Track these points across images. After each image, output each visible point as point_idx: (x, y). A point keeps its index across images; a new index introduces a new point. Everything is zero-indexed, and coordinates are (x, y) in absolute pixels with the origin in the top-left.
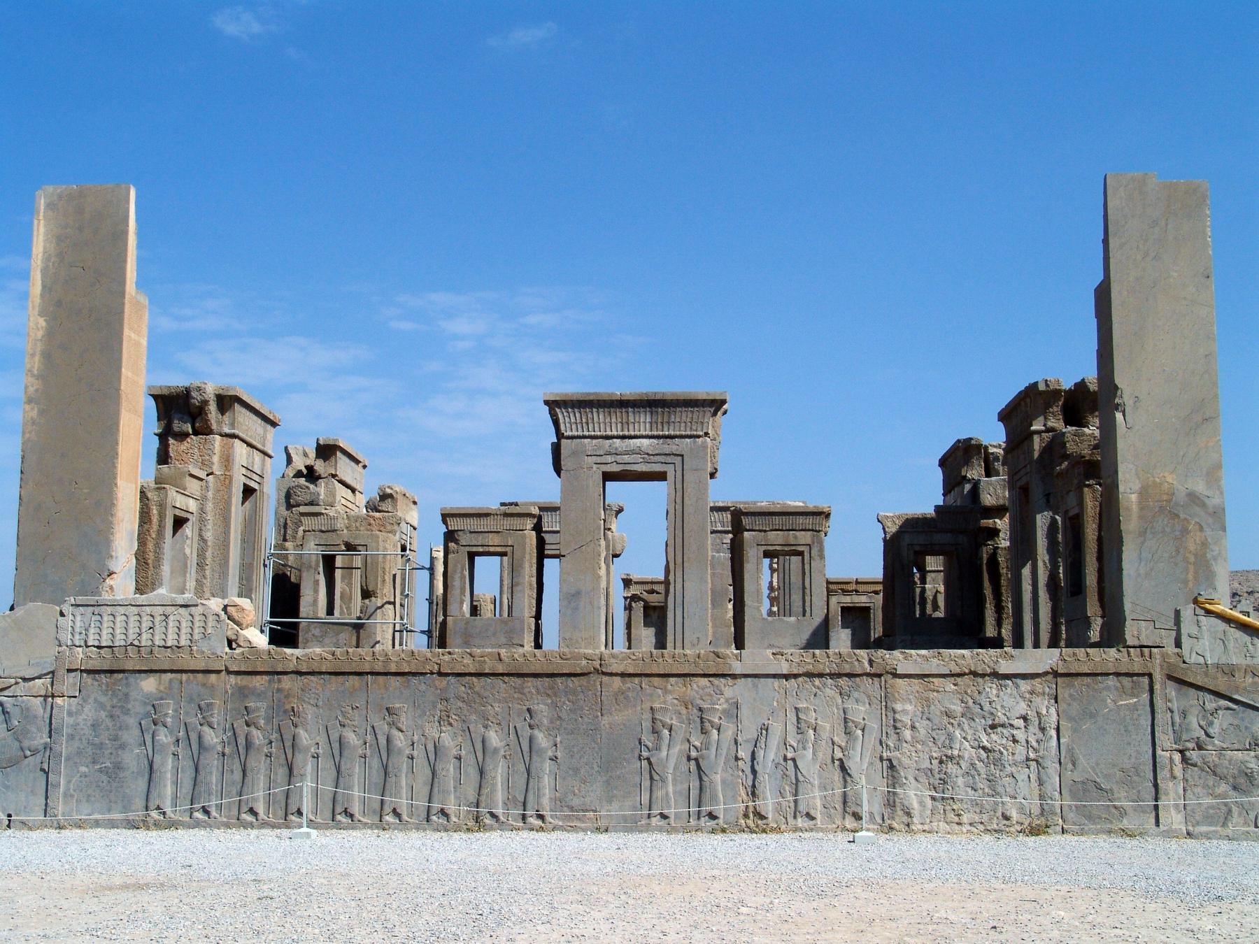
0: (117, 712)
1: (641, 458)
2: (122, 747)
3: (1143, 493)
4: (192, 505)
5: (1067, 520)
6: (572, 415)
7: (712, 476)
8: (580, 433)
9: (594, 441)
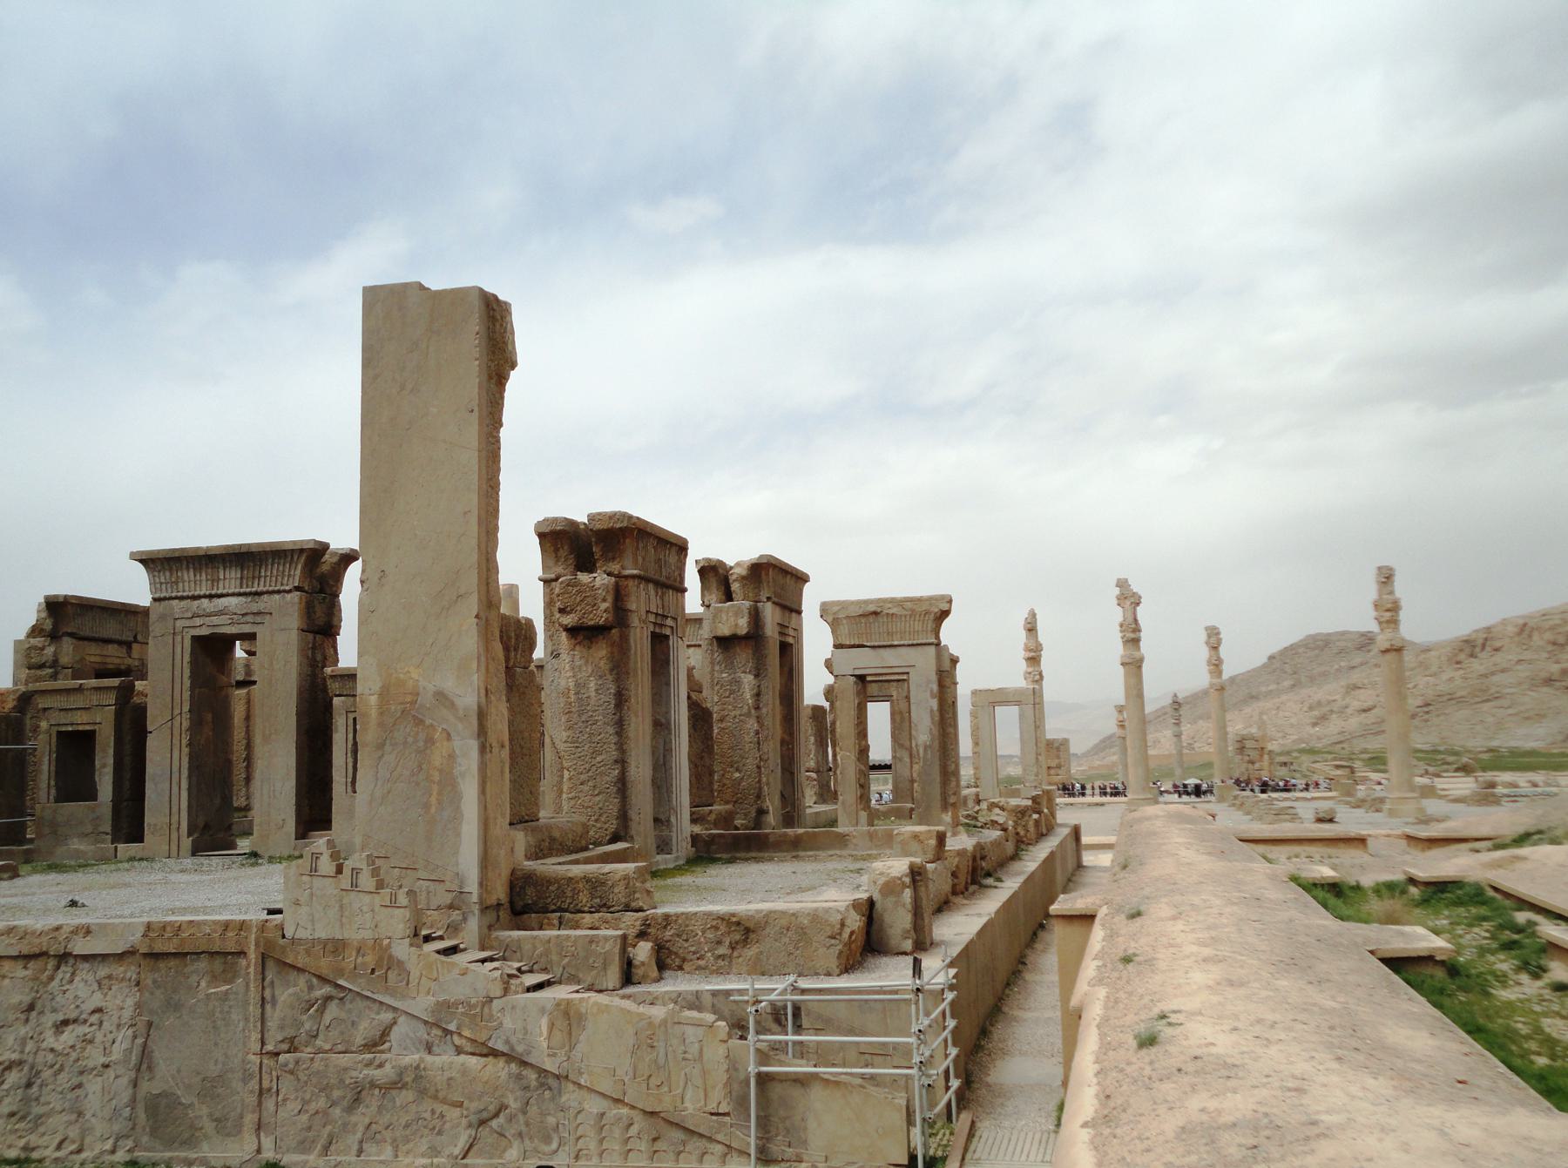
3: (384, 694)
8: (168, 596)
9: (184, 603)
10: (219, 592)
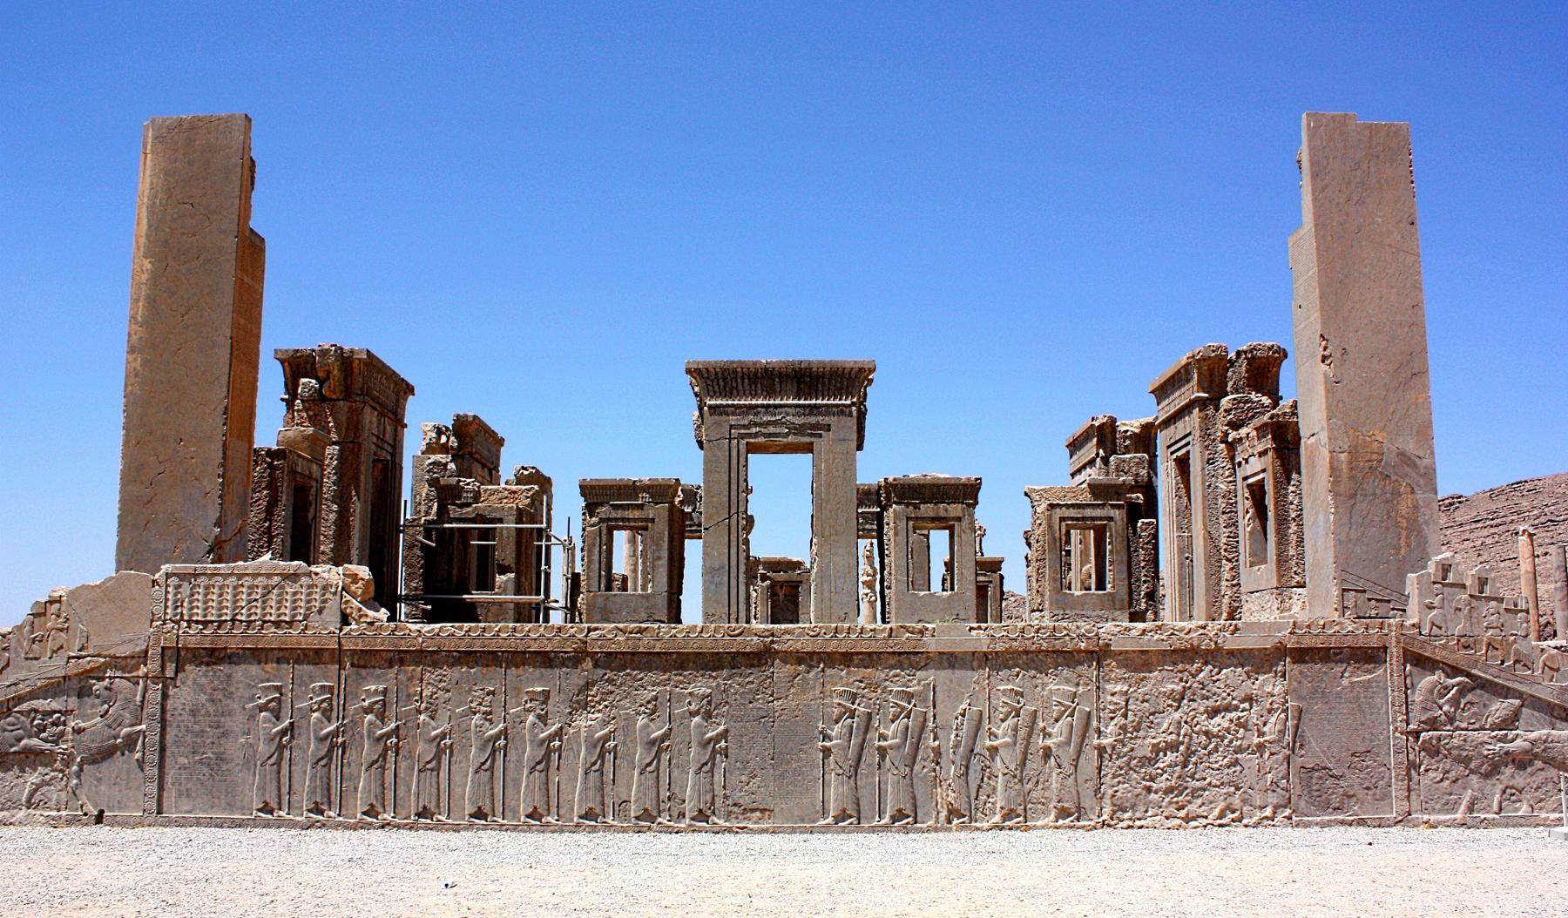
0: (219, 695)
2: (225, 735)
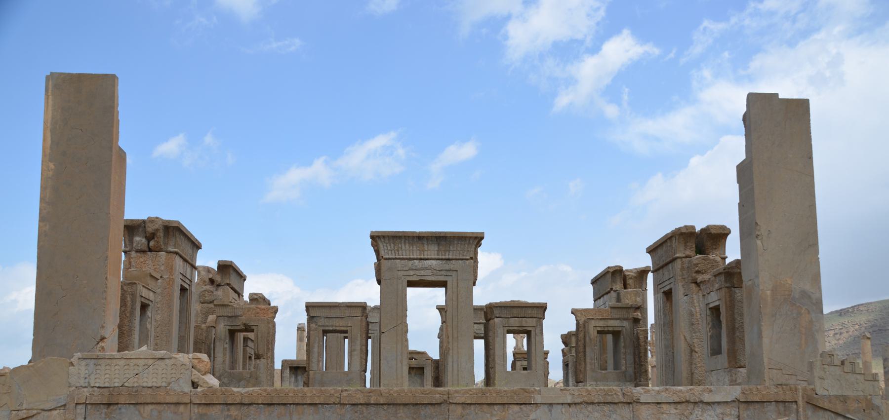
1: (433, 273)
4: (151, 296)
5: (708, 310)
6: (388, 245)
7: (474, 284)
8: (394, 257)
9: (403, 262)
10: (426, 257)
